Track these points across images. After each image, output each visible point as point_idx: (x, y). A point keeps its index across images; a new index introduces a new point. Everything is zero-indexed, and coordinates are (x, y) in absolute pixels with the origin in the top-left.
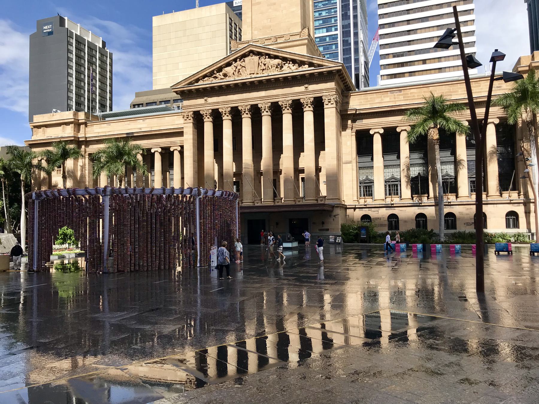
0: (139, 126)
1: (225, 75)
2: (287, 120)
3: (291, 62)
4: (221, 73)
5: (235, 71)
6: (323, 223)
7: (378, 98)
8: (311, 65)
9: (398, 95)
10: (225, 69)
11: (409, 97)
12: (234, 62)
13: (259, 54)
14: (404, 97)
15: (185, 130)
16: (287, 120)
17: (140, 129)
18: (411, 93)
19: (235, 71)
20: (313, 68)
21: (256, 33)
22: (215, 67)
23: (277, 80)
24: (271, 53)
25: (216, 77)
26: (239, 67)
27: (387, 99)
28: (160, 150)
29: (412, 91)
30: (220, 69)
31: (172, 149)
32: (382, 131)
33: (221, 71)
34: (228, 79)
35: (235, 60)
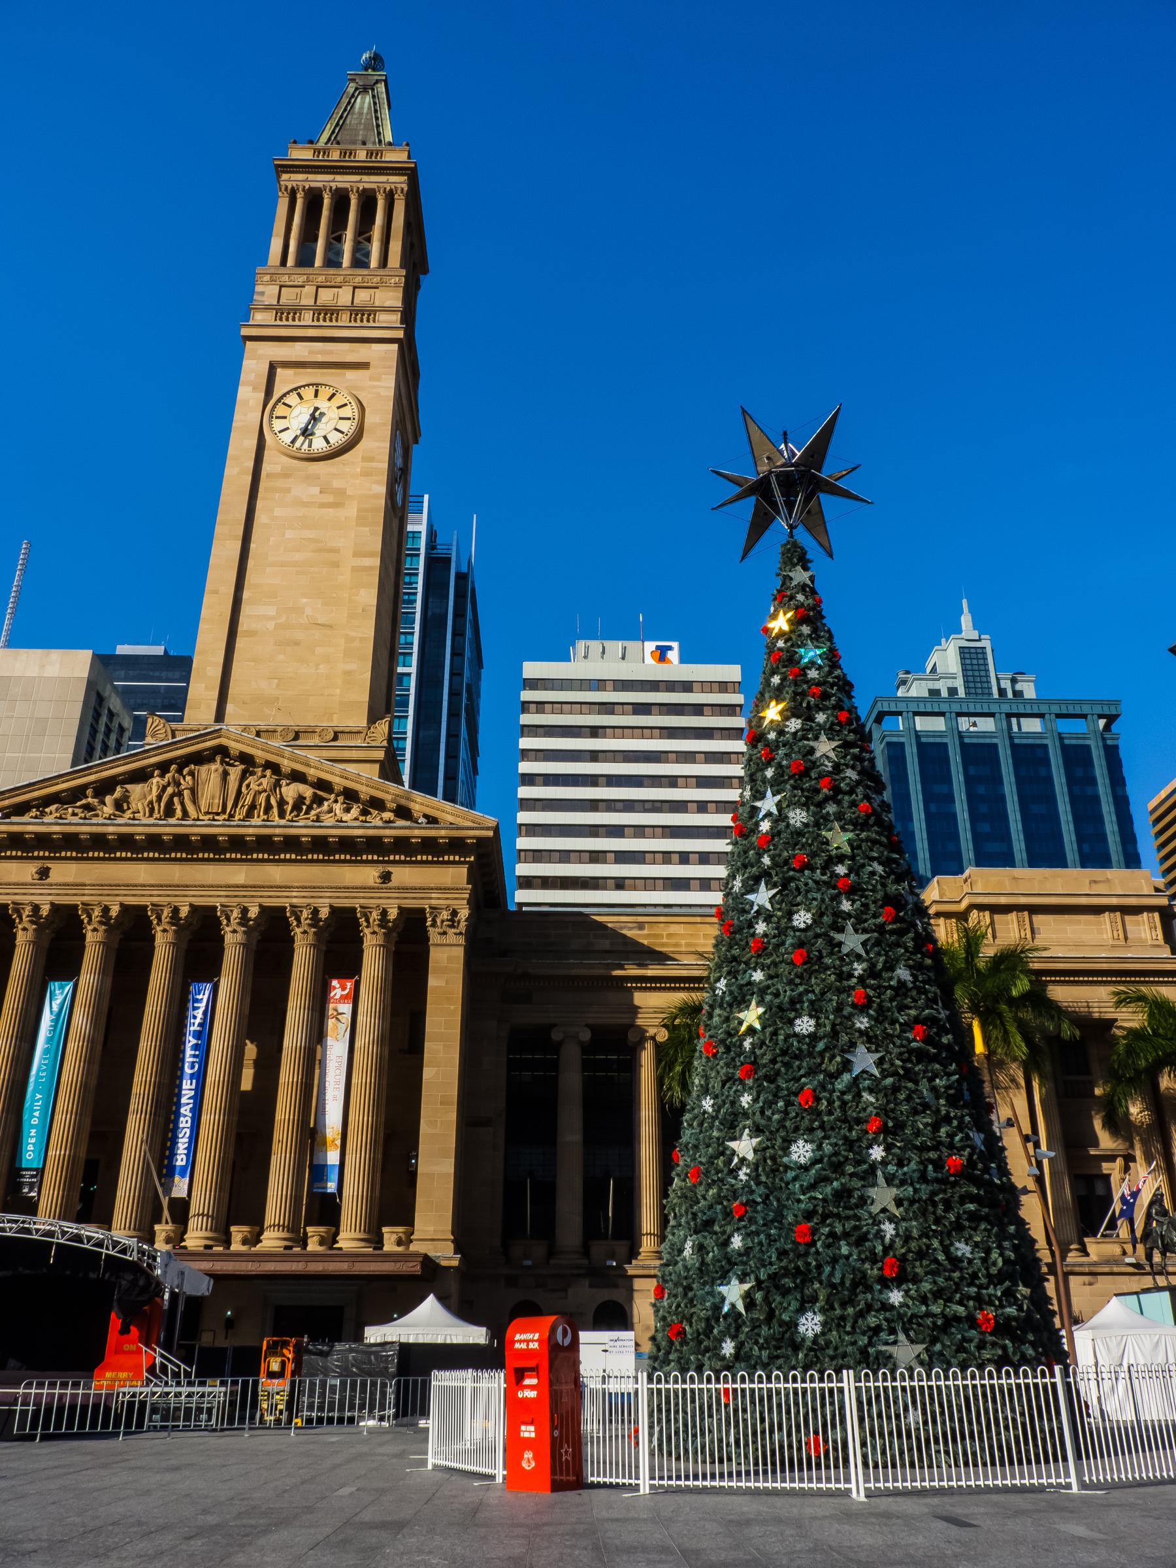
3: (341, 799)
5: (159, 798)
10: (127, 786)
13: (246, 759)
18: (670, 935)
20: (408, 823)
21: (230, 708)
22: (92, 778)
23: (292, 844)
24: (286, 762)
25: (88, 808)
29: (674, 929)
32: (586, 1036)
33: (111, 791)
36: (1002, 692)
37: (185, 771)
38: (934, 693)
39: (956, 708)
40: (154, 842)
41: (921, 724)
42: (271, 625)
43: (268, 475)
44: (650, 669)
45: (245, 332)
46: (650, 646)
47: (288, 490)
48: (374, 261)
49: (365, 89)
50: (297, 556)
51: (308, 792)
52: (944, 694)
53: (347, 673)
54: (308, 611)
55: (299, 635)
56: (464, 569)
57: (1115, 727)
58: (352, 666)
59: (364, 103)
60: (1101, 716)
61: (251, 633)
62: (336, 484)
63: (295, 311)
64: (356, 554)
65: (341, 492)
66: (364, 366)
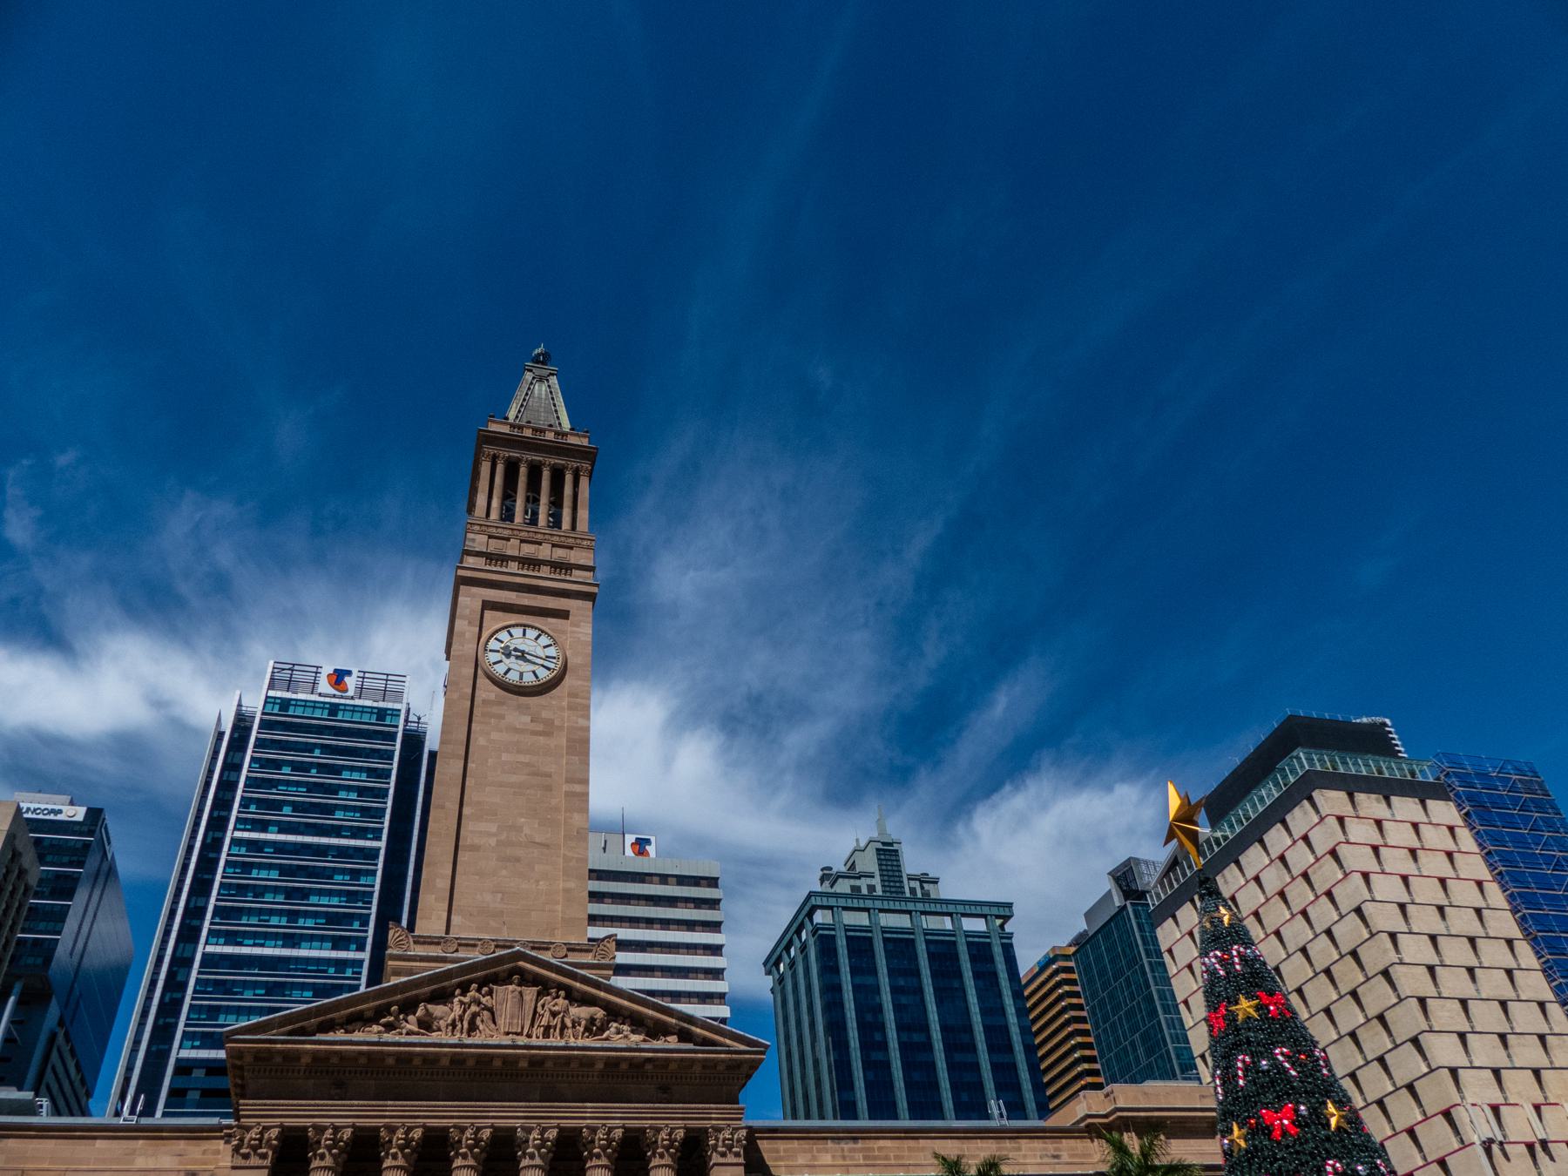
1: (426, 1025)
4: (411, 1018)
7: (805, 1151)
8: (685, 1036)
9: (851, 1150)
11: (875, 1158)
12: (458, 992)
13: (535, 980)
14: (865, 1158)
18: (880, 1149)
19: (461, 1020)
20: (690, 1046)
21: (455, 919)
25: (390, 1027)
29: (882, 1143)
30: (408, 1007)
34: (434, 1037)
36: (913, 891)
37: (485, 989)
38: (856, 889)
39: (878, 904)
41: (850, 918)
42: (493, 841)
45: (461, 573)
47: (502, 717)
48: (566, 524)
49: (541, 379)
50: (514, 779)
51: (599, 1013)
52: (865, 891)
53: (566, 891)
54: (526, 830)
55: (519, 852)
56: (436, 748)
57: (1008, 928)
58: (572, 885)
59: (540, 389)
60: (998, 917)
61: (474, 848)
62: (544, 714)
63: (503, 559)
64: (568, 781)
65: (549, 723)
66: (564, 615)
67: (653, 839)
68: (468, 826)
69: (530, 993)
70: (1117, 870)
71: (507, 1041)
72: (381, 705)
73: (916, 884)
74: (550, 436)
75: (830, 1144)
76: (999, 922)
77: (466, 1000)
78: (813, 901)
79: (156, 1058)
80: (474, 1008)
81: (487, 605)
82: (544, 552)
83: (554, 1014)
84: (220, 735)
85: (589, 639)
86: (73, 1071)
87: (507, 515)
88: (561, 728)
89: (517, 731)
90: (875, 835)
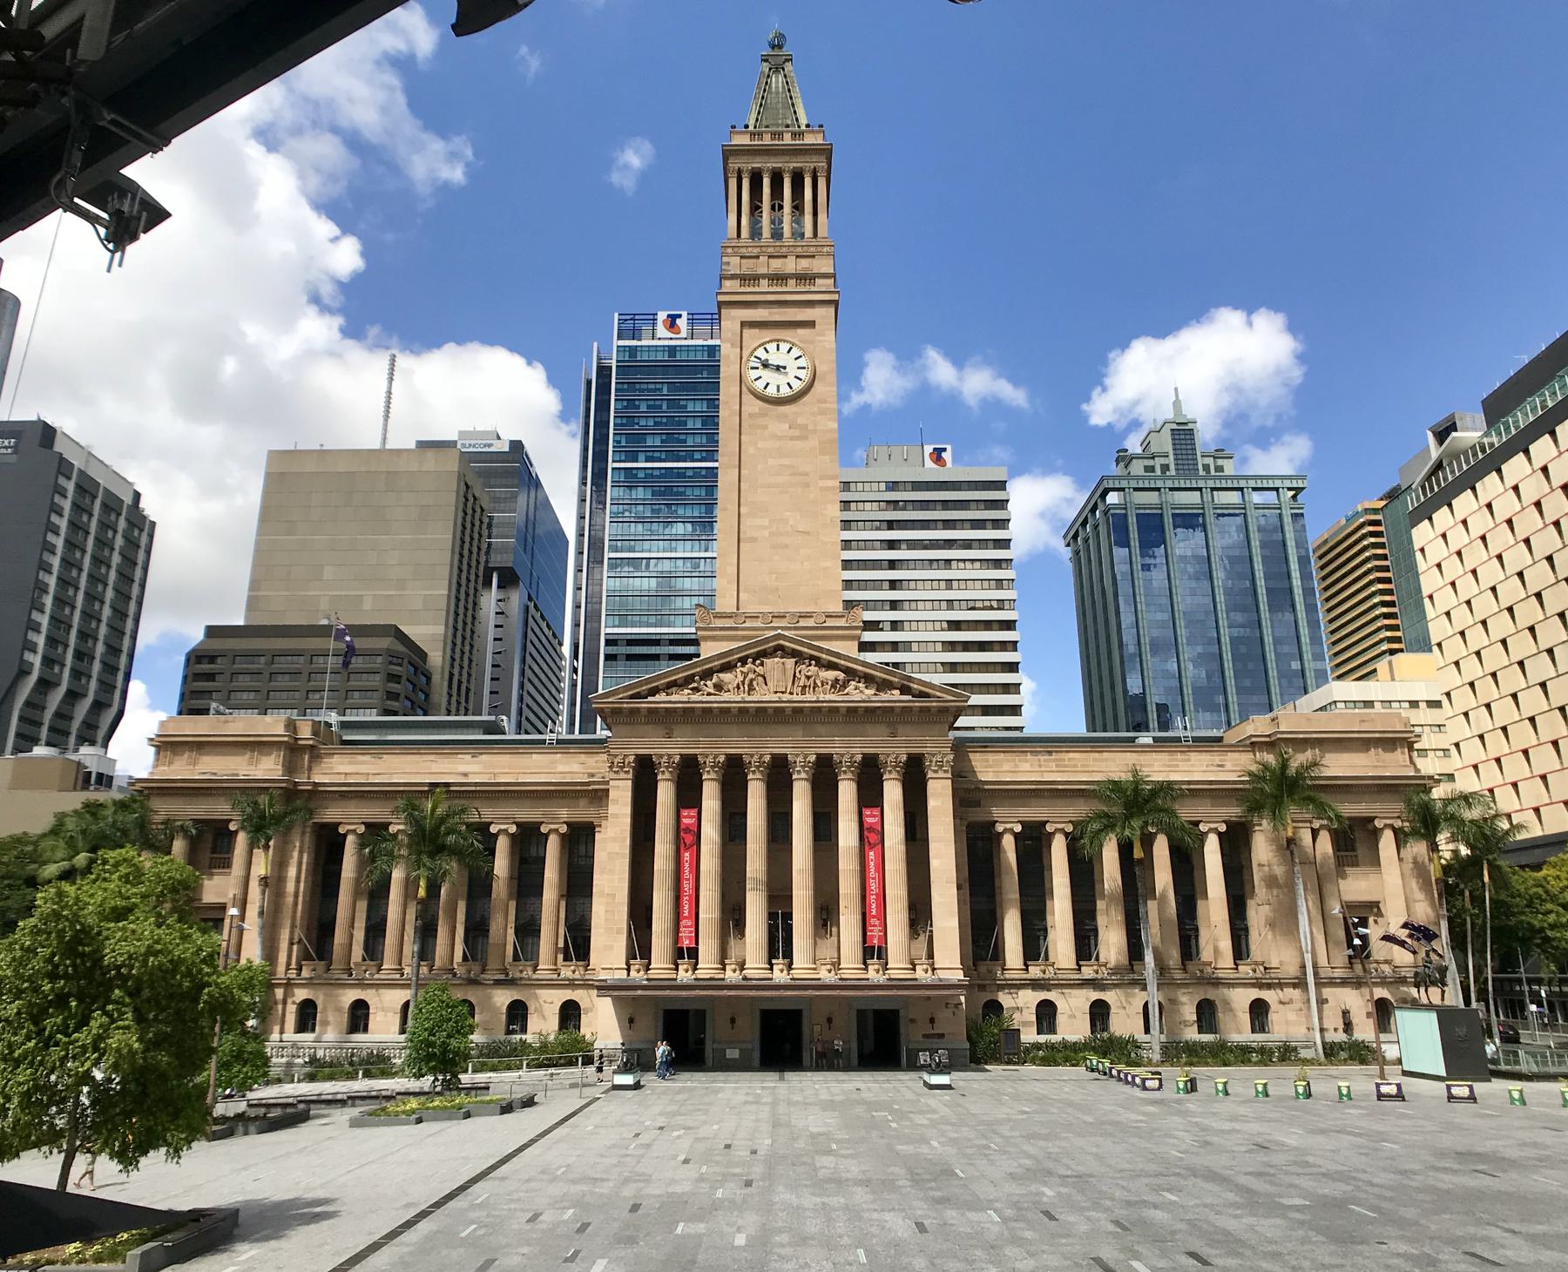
0: (462, 768)
1: (719, 687)
2: (847, 792)
6: (932, 1021)
8: (905, 690)
13: (794, 654)
15: (611, 793)
16: (847, 792)
17: (466, 775)
25: (696, 690)
26: (751, 676)
27: (1026, 766)
28: (513, 829)
29: (1071, 755)
30: (707, 675)
31: (544, 829)
34: (725, 697)
35: (743, 661)
36: (1206, 468)
40: (743, 711)
42: (766, 533)
43: (751, 415)
44: (931, 472)
45: (721, 298)
46: (929, 449)
47: (766, 427)
51: (841, 676)
54: (791, 522)
60: (1290, 489)
61: (753, 540)
63: (754, 278)
66: (810, 324)
67: (949, 447)
68: (745, 522)
69: (790, 662)
70: (1439, 425)
71: (775, 697)
72: (711, 342)
73: (1210, 461)
74: (787, 139)
75: (1029, 756)
76: (1291, 493)
77: (745, 670)
78: (1106, 484)
79: (592, 635)
80: (751, 676)
81: (743, 324)
82: (790, 265)
83: (808, 678)
84: (589, 383)
85: (833, 345)
86: (546, 629)
87: (755, 233)
88: (815, 431)
89: (780, 438)
90: (1170, 416)
